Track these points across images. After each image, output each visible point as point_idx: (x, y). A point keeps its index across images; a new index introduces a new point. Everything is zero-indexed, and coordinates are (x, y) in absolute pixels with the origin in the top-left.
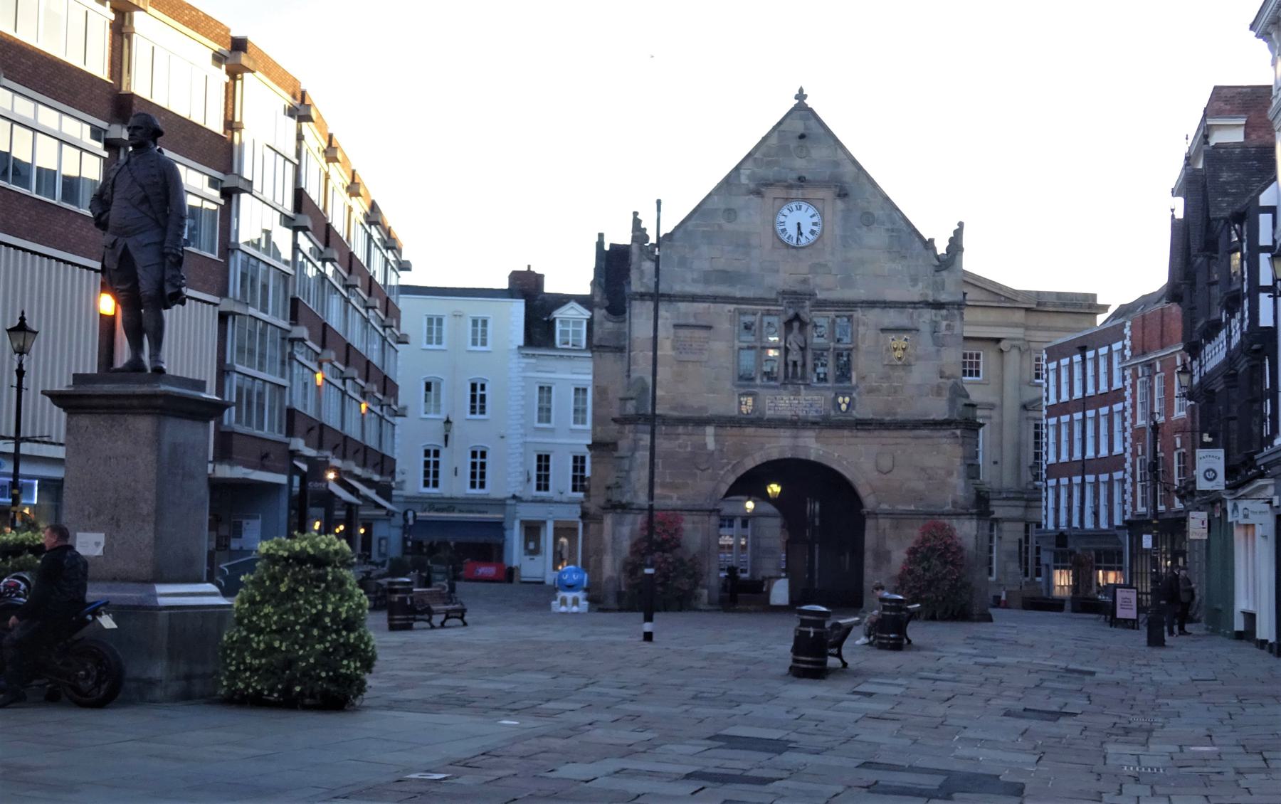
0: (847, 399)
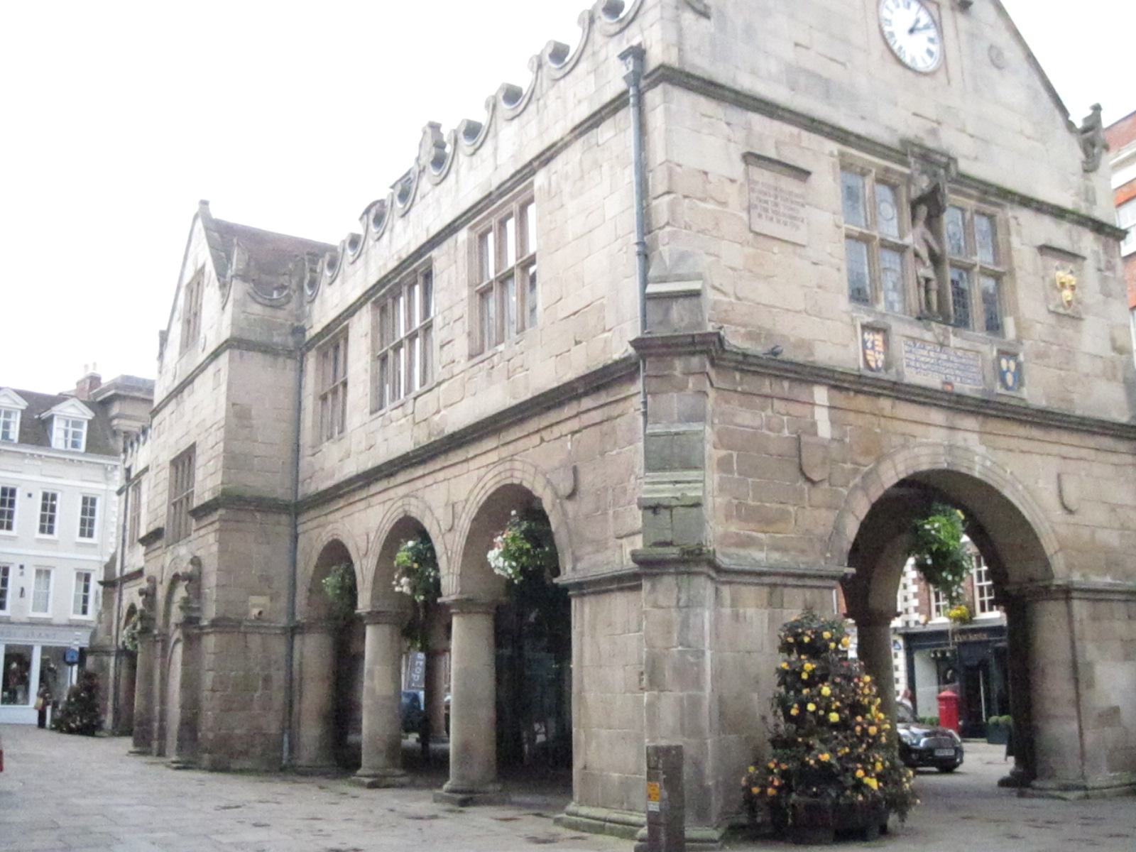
0: (1012, 365)
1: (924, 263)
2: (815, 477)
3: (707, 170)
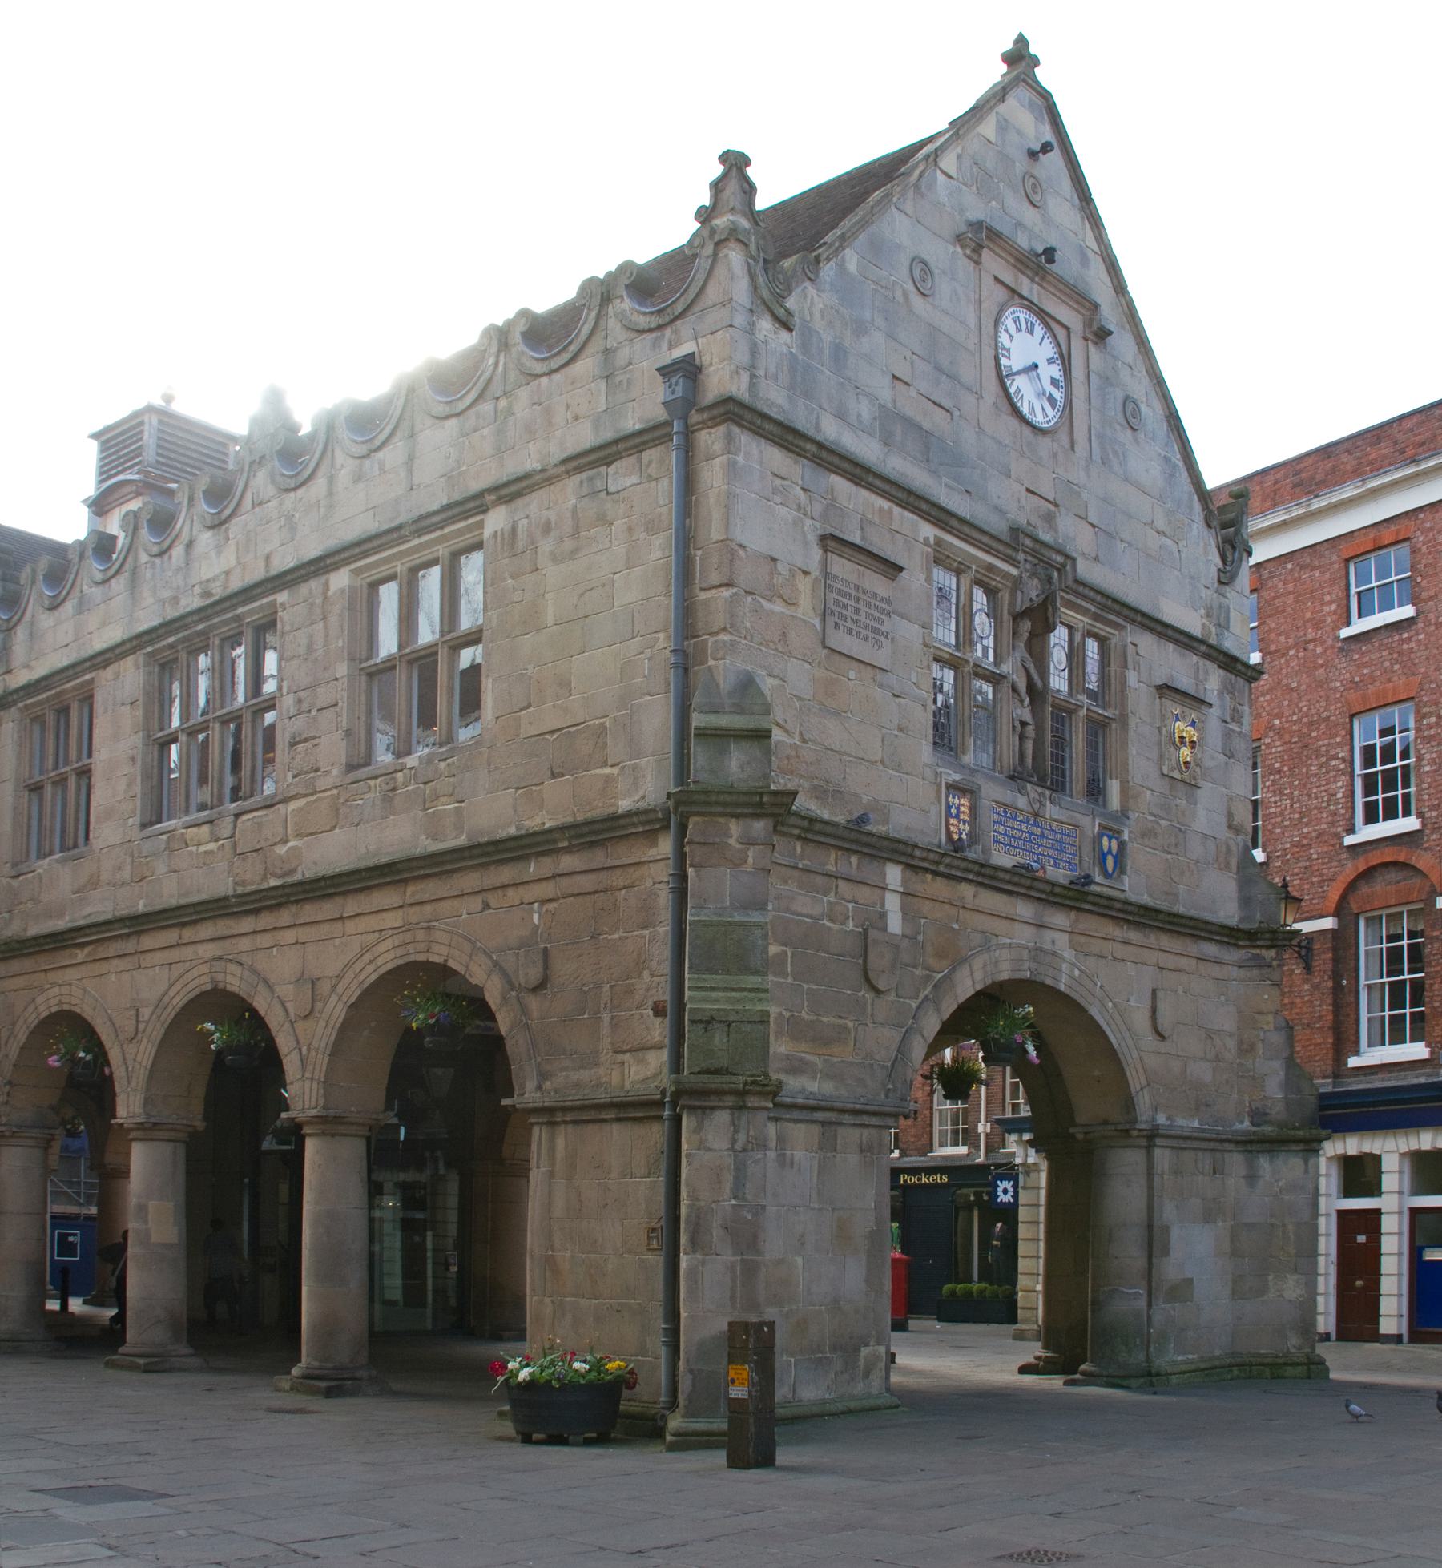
0: (1114, 843)
1: (1022, 701)
2: (881, 987)
3: (775, 555)
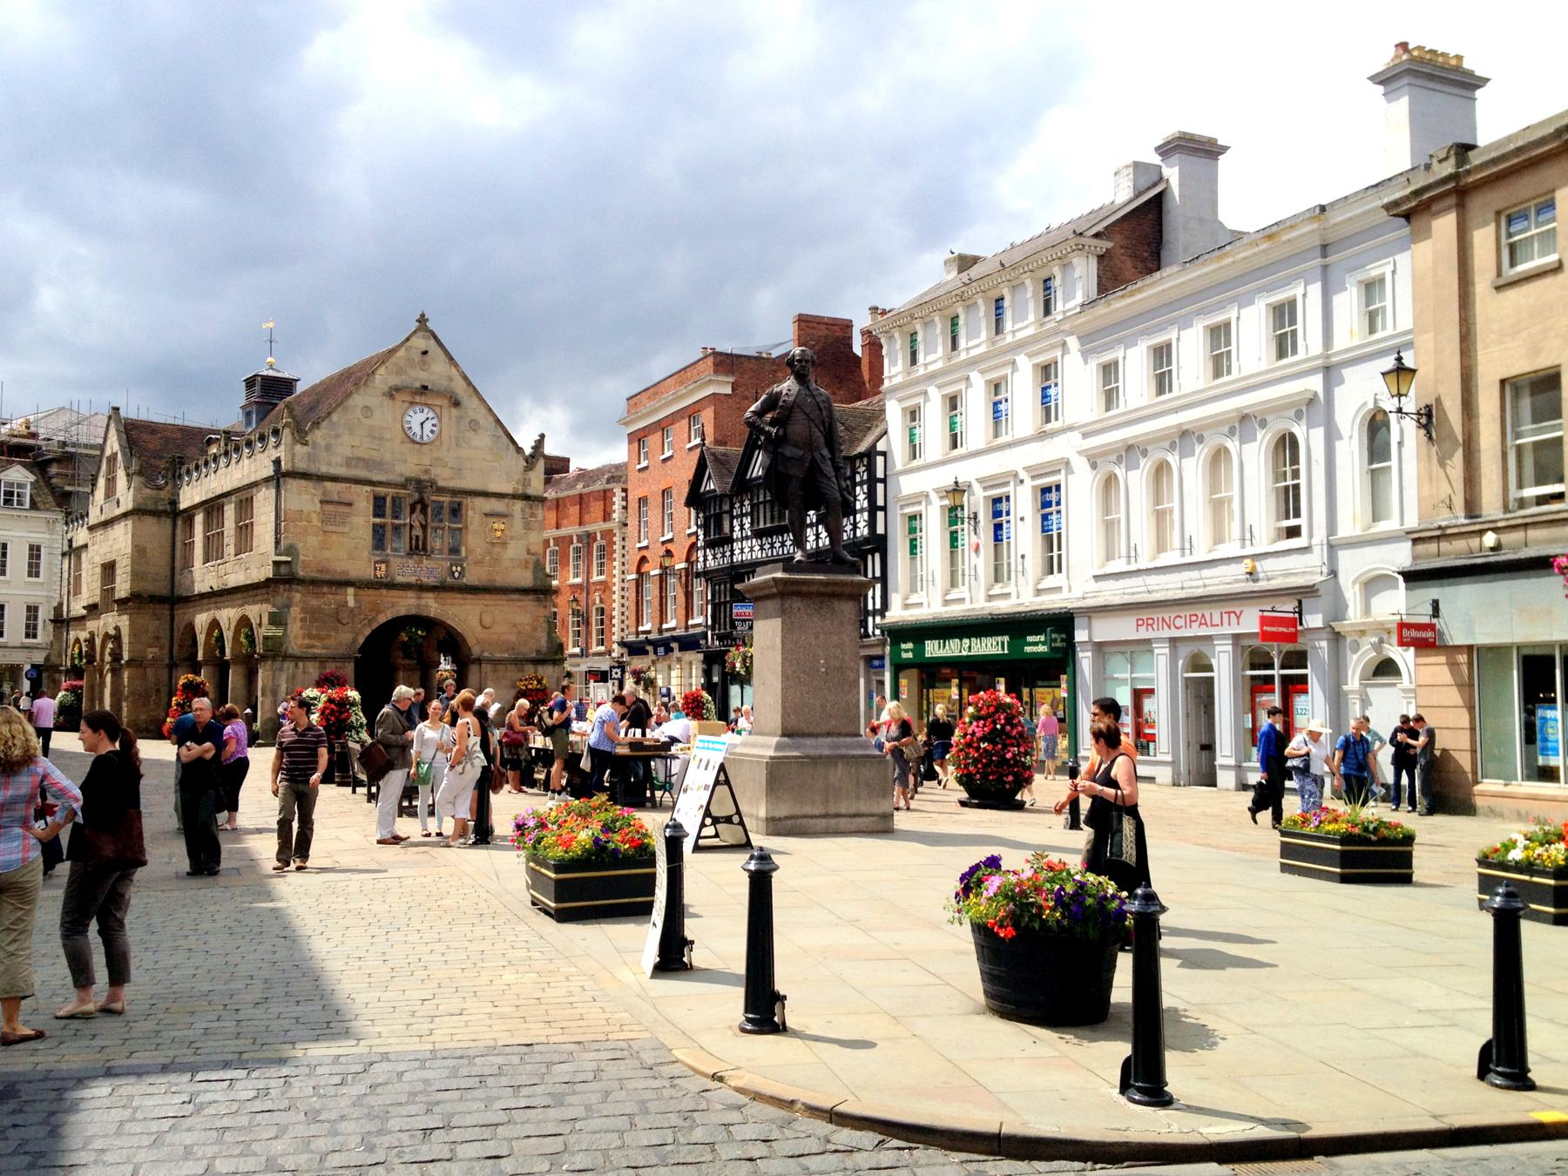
0: (459, 569)
2: (344, 622)
